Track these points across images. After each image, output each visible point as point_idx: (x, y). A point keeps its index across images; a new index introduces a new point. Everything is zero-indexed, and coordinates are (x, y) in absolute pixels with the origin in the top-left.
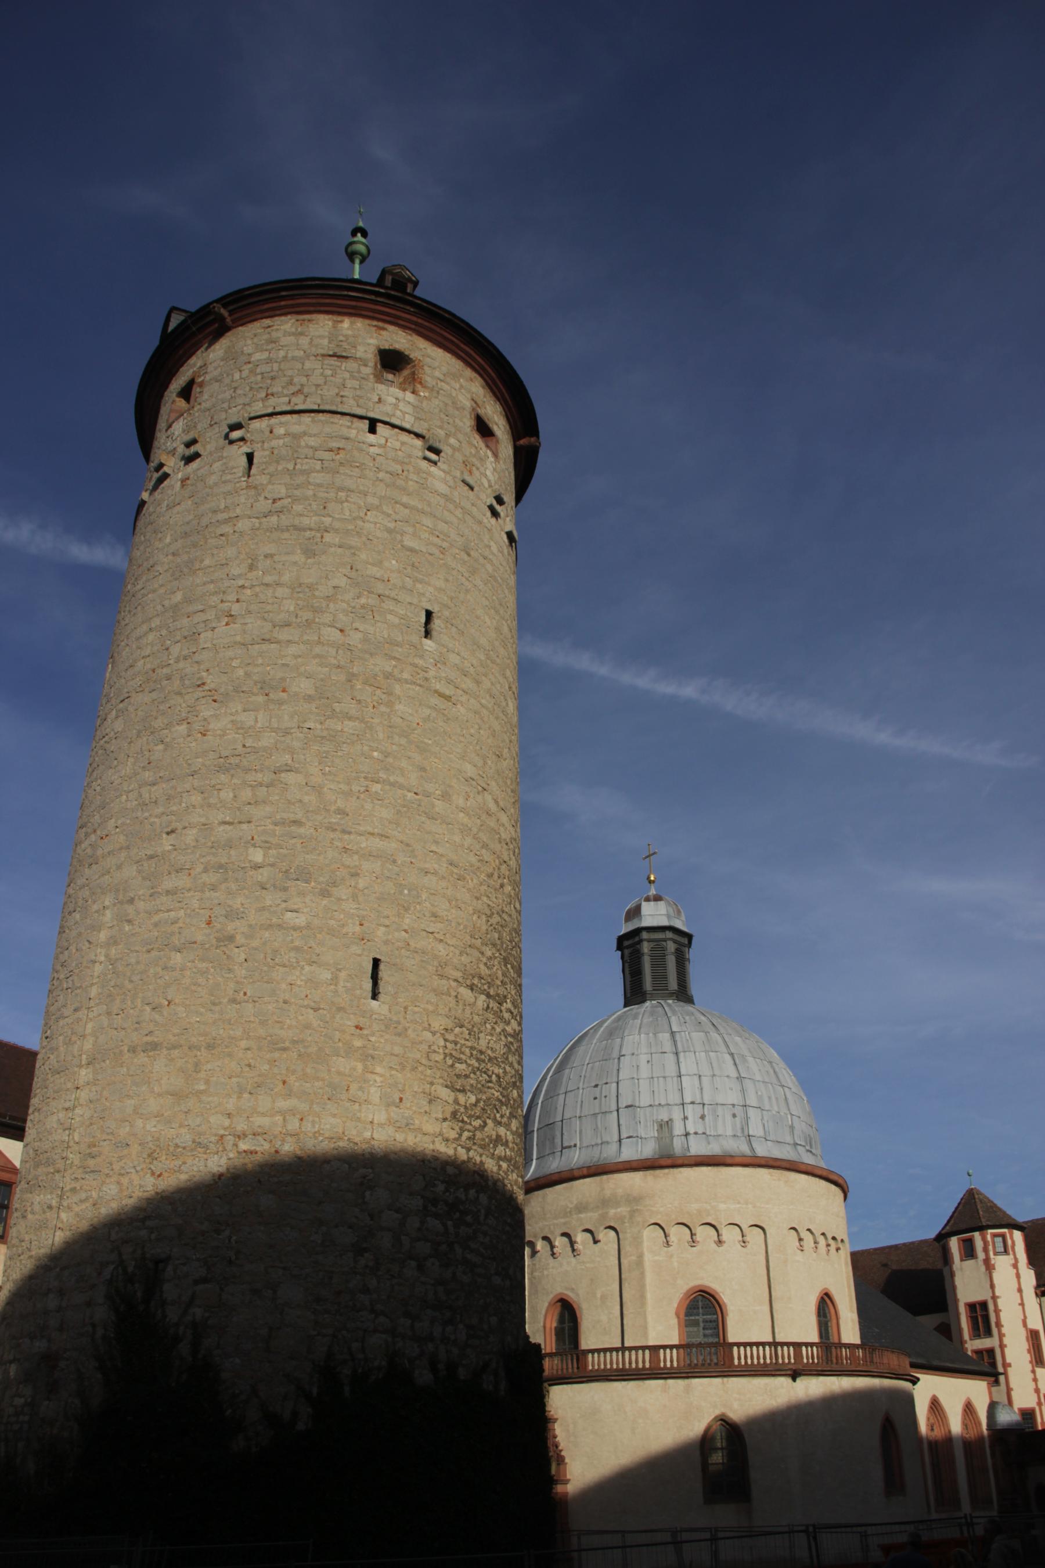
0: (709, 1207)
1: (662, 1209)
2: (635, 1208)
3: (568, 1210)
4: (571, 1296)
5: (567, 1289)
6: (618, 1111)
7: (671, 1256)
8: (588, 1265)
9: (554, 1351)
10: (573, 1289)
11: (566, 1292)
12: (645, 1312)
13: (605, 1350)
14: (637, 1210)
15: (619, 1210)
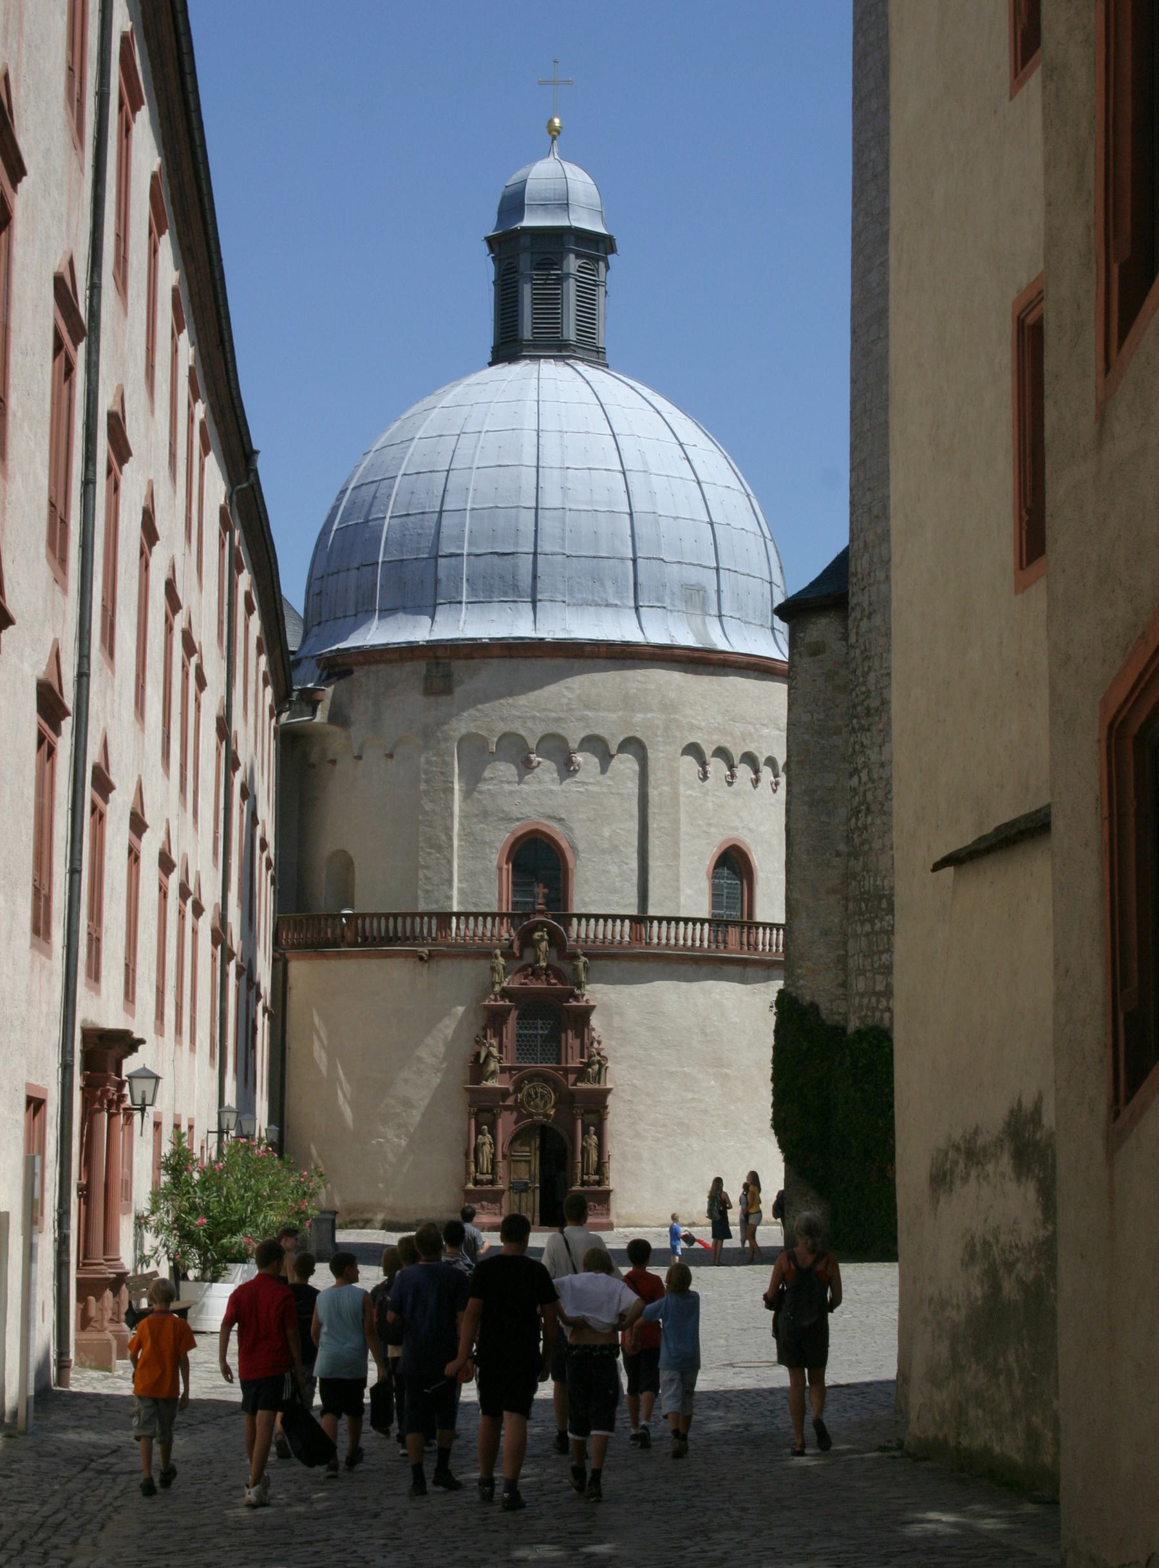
0: (753, 730)
1: (703, 724)
2: (672, 716)
3: (565, 701)
4: (555, 830)
5: (550, 817)
6: (634, 561)
7: (706, 794)
8: (590, 788)
9: (504, 910)
10: (562, 820)
11: (546, 822)
12: (678, 866)
13: (606, 917)
14: (674, 719)
15: (649, 715)
